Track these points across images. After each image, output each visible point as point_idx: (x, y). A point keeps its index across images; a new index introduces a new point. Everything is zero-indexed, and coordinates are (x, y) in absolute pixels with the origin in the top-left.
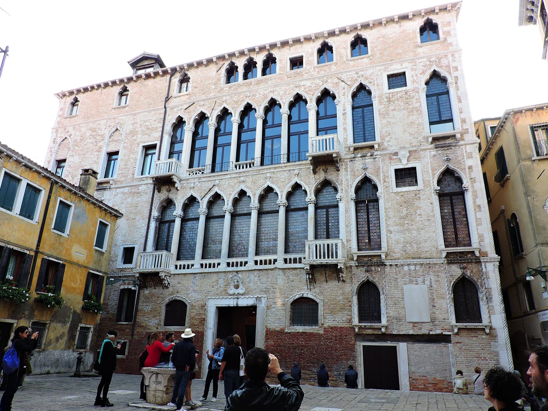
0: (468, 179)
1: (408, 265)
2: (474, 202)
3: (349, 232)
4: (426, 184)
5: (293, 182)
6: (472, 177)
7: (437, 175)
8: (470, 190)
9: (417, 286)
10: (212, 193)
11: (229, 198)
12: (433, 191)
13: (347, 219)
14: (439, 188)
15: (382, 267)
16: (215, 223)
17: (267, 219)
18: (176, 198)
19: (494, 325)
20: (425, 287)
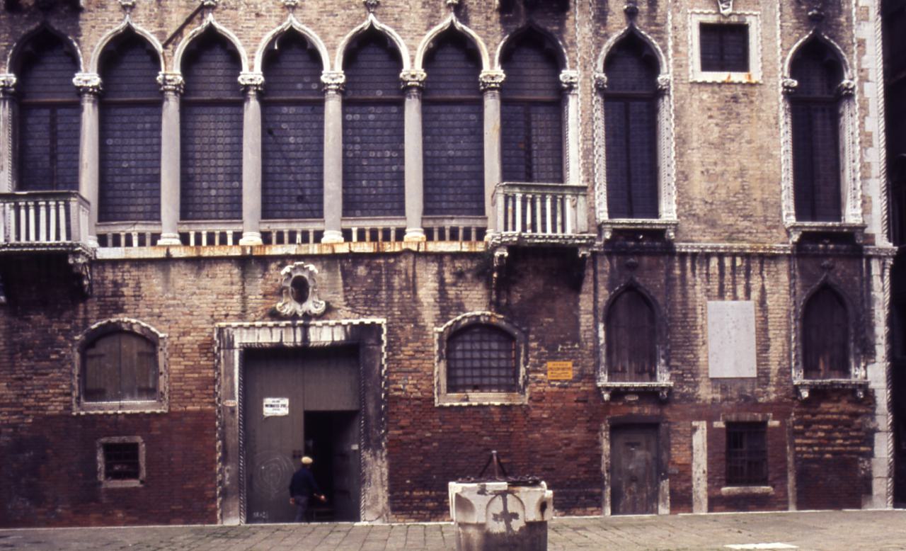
0: (855, 71)
1: (721, 256)
2: (862, 125)
3: (589, 171)
4: (767, 74)
5: (443, 24)
6: (864, 66)
7: (791, 52)
8: (857, 98)
9: (735, 303)
10: (197, 29)
11: (253, 52)
12: (781, 90)
13: (588, 138)
14: (795, 83)
15: (667, 257)
16: (205, 118)
17: (211, 125)
18: (77, 32)
19: (872, 386)
20: (751, 306)
